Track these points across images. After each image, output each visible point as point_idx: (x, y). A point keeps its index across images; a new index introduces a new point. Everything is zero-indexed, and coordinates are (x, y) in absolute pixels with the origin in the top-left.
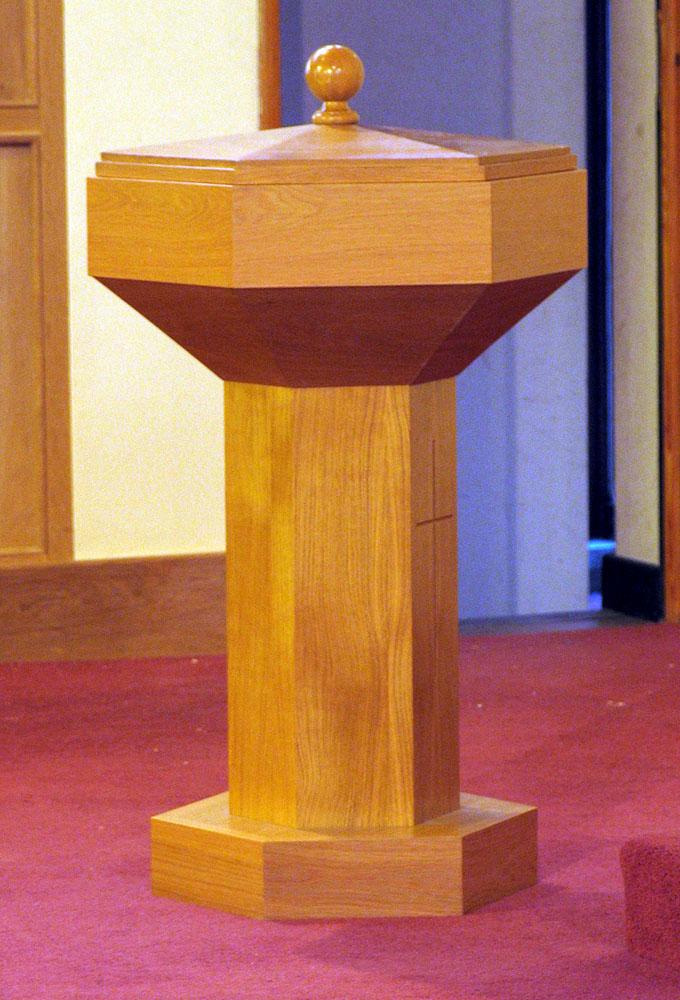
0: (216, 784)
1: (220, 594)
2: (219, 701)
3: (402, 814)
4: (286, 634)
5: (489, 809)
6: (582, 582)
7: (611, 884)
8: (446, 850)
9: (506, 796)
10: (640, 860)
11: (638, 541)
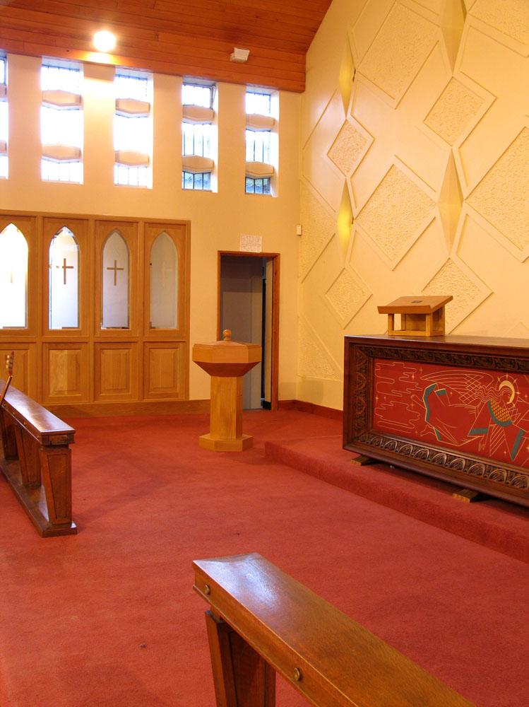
0: (207, 432)
1: (209, 404)
2: (209, 420)
3: (234, 437)
4: (219, 412)
5: (246, 436)
6: (260, 404)
7: (262, 446)
8: (240, 442)
9: (249, 434)
10: (268, 444)
11: (268, 399)
